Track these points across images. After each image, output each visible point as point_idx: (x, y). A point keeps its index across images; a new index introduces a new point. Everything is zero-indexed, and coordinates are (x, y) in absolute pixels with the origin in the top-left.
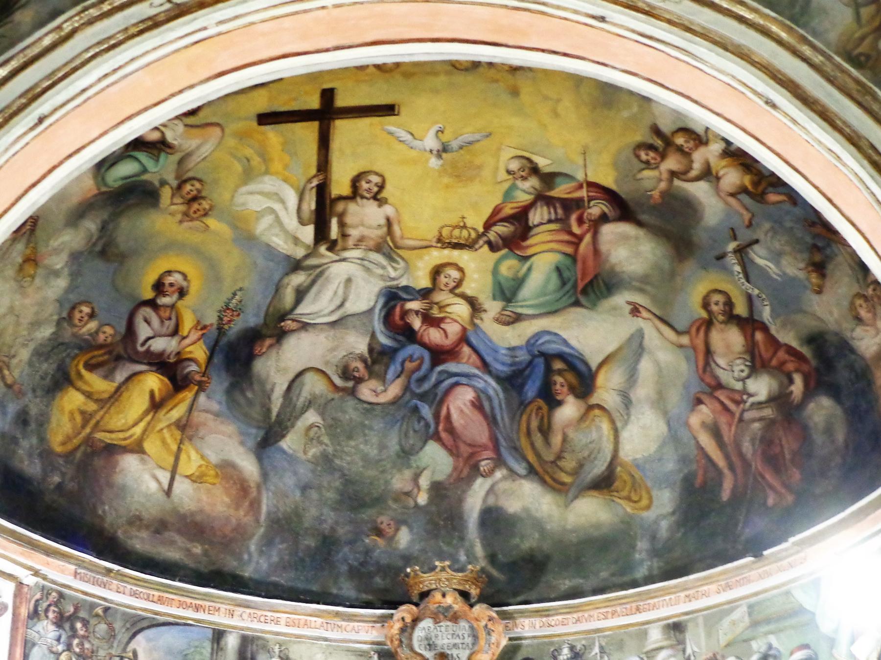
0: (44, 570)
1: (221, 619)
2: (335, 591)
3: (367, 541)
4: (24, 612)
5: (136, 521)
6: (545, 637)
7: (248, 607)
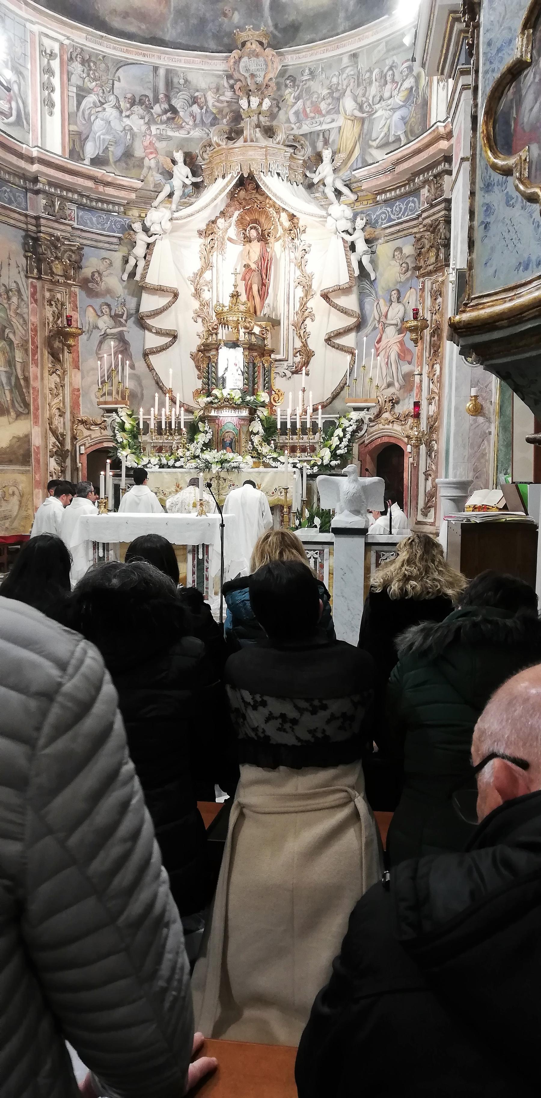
0: (72, 37)
1: (155, 61)
2: (206, 46)
3: (220, 20)
4: (65, 58)
5: (114, 12)
6: (298, 64)
7: (167, 54)
